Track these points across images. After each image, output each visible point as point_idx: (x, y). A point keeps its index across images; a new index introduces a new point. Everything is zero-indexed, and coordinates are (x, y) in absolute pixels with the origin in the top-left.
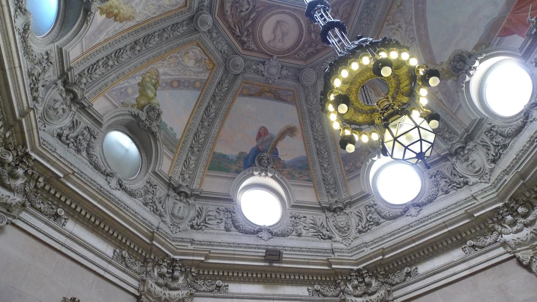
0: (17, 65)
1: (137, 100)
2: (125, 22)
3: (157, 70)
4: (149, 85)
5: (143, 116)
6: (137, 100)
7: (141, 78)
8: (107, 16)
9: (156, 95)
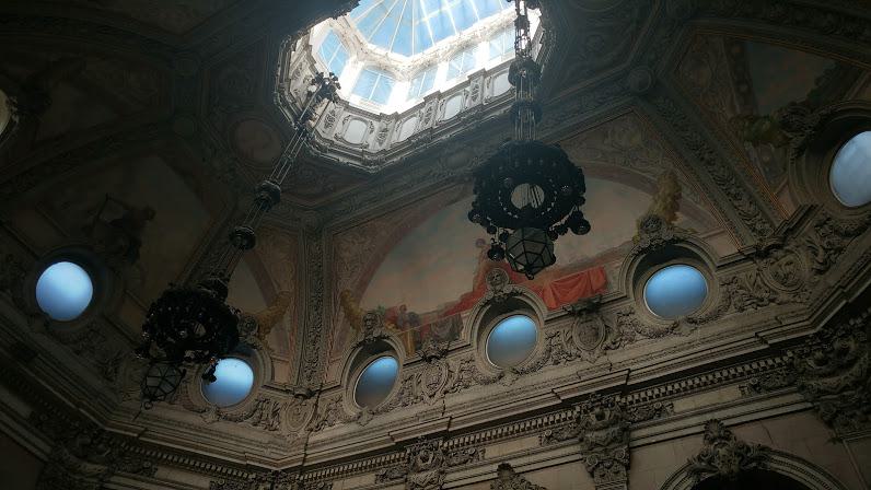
0: (709, 352)
1: (778, 147)
2: (680, 184)
3: (730, 122)
4: (753, 129)
5: (798, 140)
6: (778, 147)
7: (746, 144)
8: (677, 210)
9: (766, 117)
